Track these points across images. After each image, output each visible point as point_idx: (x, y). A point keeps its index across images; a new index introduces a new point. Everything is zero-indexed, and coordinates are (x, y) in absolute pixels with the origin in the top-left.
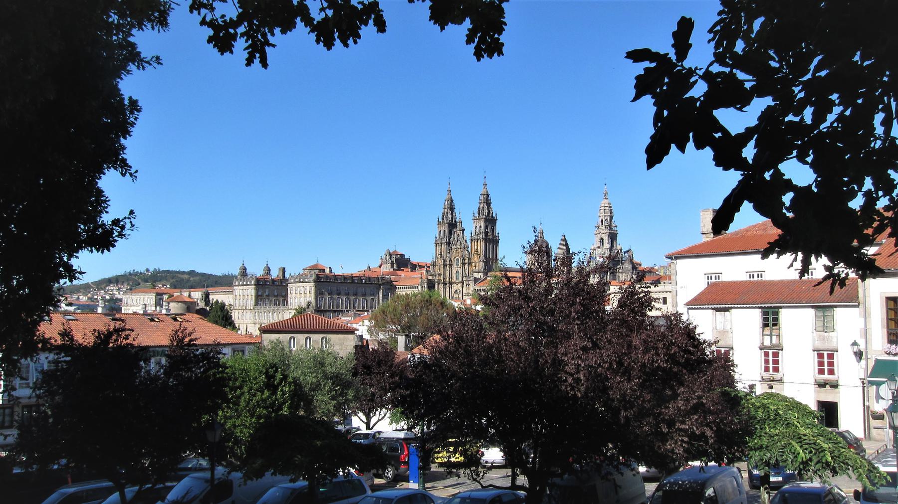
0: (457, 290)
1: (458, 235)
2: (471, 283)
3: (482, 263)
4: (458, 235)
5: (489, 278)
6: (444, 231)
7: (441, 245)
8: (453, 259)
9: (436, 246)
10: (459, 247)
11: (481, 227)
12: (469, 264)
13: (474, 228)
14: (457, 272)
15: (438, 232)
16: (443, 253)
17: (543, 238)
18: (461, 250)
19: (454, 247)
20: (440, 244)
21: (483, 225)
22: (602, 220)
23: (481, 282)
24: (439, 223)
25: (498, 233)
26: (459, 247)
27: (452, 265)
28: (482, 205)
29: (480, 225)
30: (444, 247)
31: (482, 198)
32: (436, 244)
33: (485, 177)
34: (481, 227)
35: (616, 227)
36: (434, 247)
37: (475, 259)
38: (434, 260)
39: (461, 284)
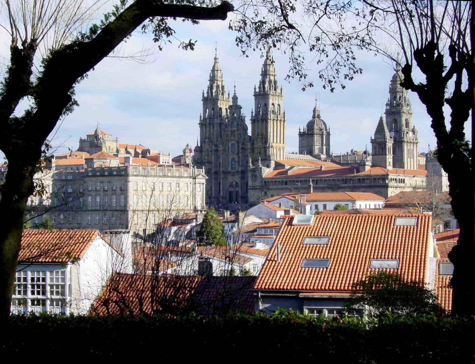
10: (235, 129)
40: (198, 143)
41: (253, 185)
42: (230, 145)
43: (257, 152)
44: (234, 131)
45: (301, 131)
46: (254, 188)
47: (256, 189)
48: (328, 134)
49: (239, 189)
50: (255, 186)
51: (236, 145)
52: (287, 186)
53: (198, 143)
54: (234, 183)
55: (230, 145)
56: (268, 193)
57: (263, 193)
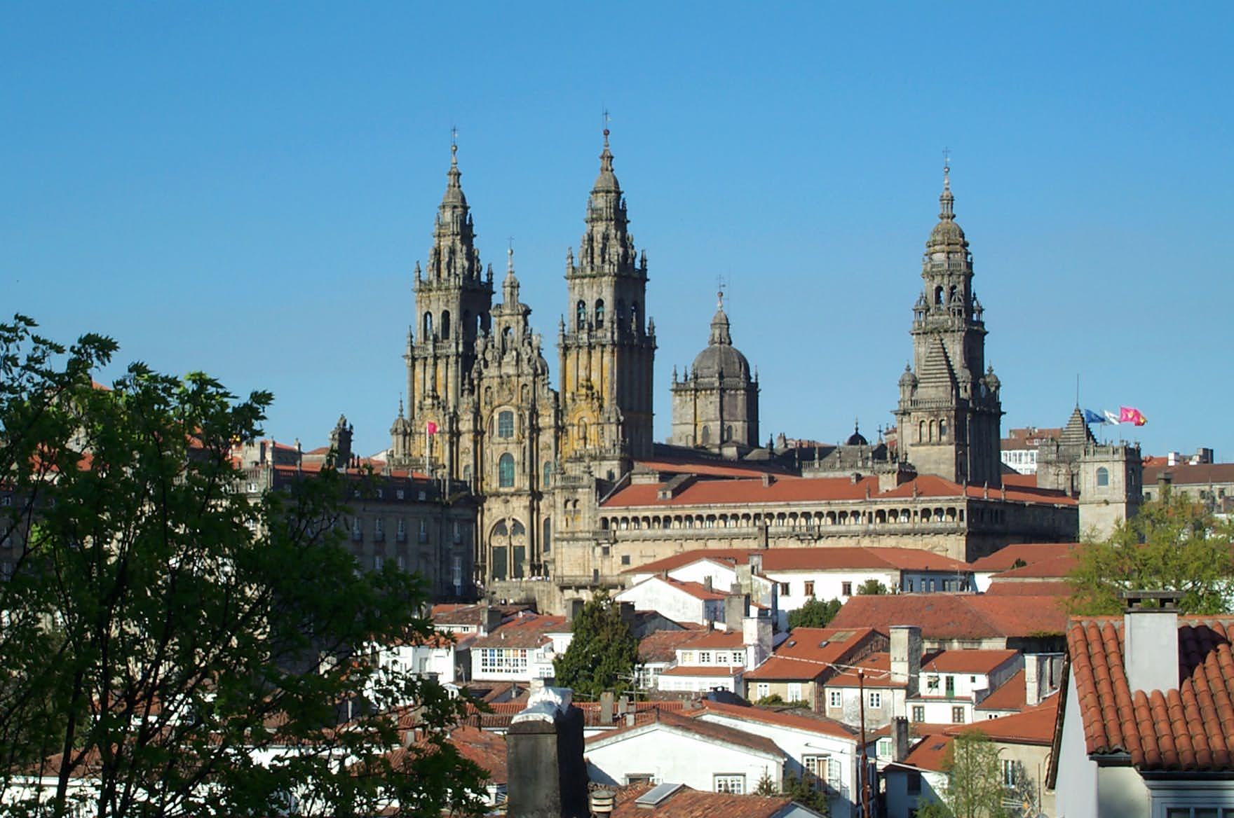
0: (504, 520)
1: (507, 329)
2: (586, 496)
3: (614, 428)
4: (507, 329)
5: (637, 480)
6: (446, 315)
7: (435, 365)
8: (485, 412)
9: (413, 366)
10: (511, 370)
11: (600, 303)
12: (560, 430)
13: (573, 306)
14: (506, 457)
15: (419, 318)
16: (441, 392)
17: (730, 343)
18: (522, 380)
19: (492, 371)
20: (430, 361)
21: (608, 297)
22: (939, 289)
23: (617, 491)
24: (425, 288)
25: (652, 328)
26: (511, 370)
27: (483, 433)
28: (600, 228)
29: (596, 297)
30: (448, 374)
31: (600, 202)
32: (414, 359)
33: (607, 133)
34: (600, 303)
35: (981, 311)
36: (407, 371)
37: (582, 413)
38: (407, 417)
39: (525, 501)
40: (401, 411)
41: (570, 529)
42: (496, 417)
43: (576, 436)
44: (509, 376)
45: (679, 381)
46: (573, 538)
47: (577, 540)
48: (752, 391)
49: (522, 540)
50: (573, 533)
51: (515, 417)
52: (668, 531)
53: (401, 411)
54: (509, 524)
55: (496, 417)
56: (613, 550)
57: (599, 550)
